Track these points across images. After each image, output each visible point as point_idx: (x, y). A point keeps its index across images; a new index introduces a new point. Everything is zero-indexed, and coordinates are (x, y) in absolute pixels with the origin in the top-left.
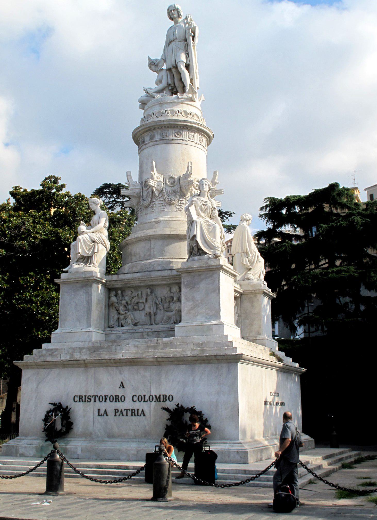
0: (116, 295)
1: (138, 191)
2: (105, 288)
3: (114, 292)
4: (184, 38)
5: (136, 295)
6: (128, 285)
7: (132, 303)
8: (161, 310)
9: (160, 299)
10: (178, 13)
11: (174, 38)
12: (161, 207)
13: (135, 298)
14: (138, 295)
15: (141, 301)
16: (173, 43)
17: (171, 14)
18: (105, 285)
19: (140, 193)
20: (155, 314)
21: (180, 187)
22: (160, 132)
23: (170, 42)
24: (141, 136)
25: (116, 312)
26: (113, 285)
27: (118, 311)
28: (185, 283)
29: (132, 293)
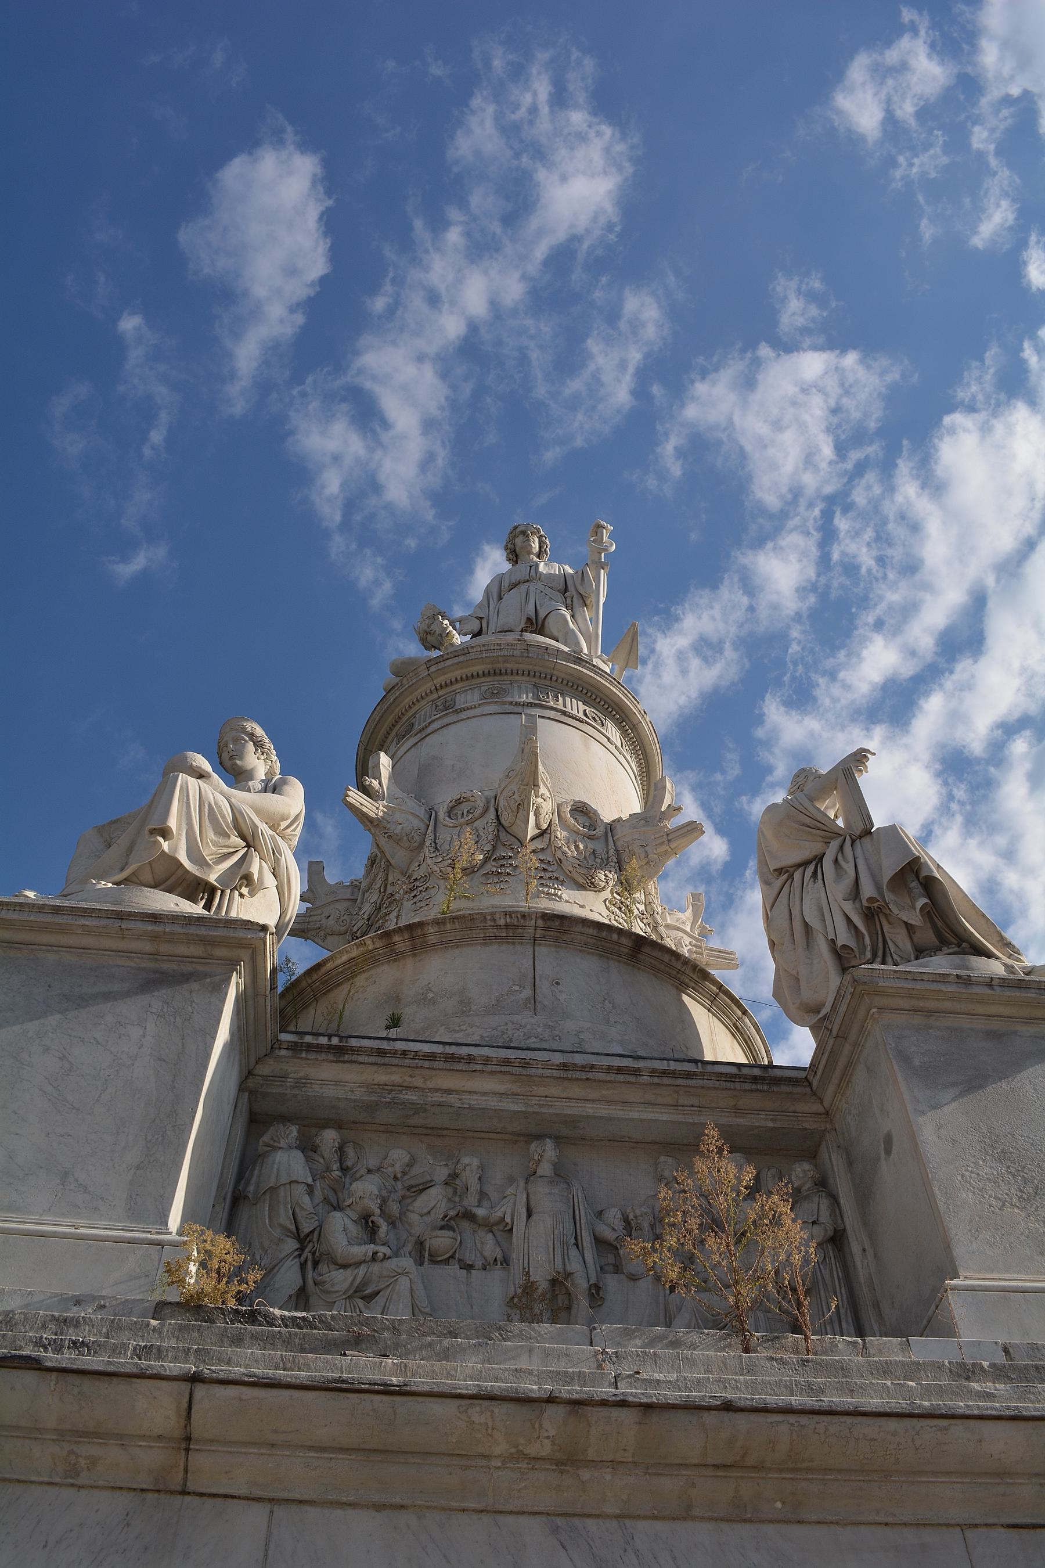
0: (308, 1147)
1: (416, 823)
2: (242, 1087)
3: (294, 1131)
4: (562, 586)
5: (442, 1173)
6: (410, 1096)
7: (414, 1217)
8: (633, 1278)
9: (613, 1216)
10: (540, 547)
11: (533, 573)
12: (544, 882)
13: (433, 1191)
14: (454, 1176)
15: (480, 1212)
16: (523, 587)
17: (519, 541)
18: (250, 1073)
19: (425, 835)
20: (596, 1293)
21: (617, 851)
22: (531, 686)
23: (514, 586)
24: (435, 696)
25: (291, 1245)
26: (302, 1083)
27: (302, 1240)
28: (917, 1062)
29: (410, 1165)
